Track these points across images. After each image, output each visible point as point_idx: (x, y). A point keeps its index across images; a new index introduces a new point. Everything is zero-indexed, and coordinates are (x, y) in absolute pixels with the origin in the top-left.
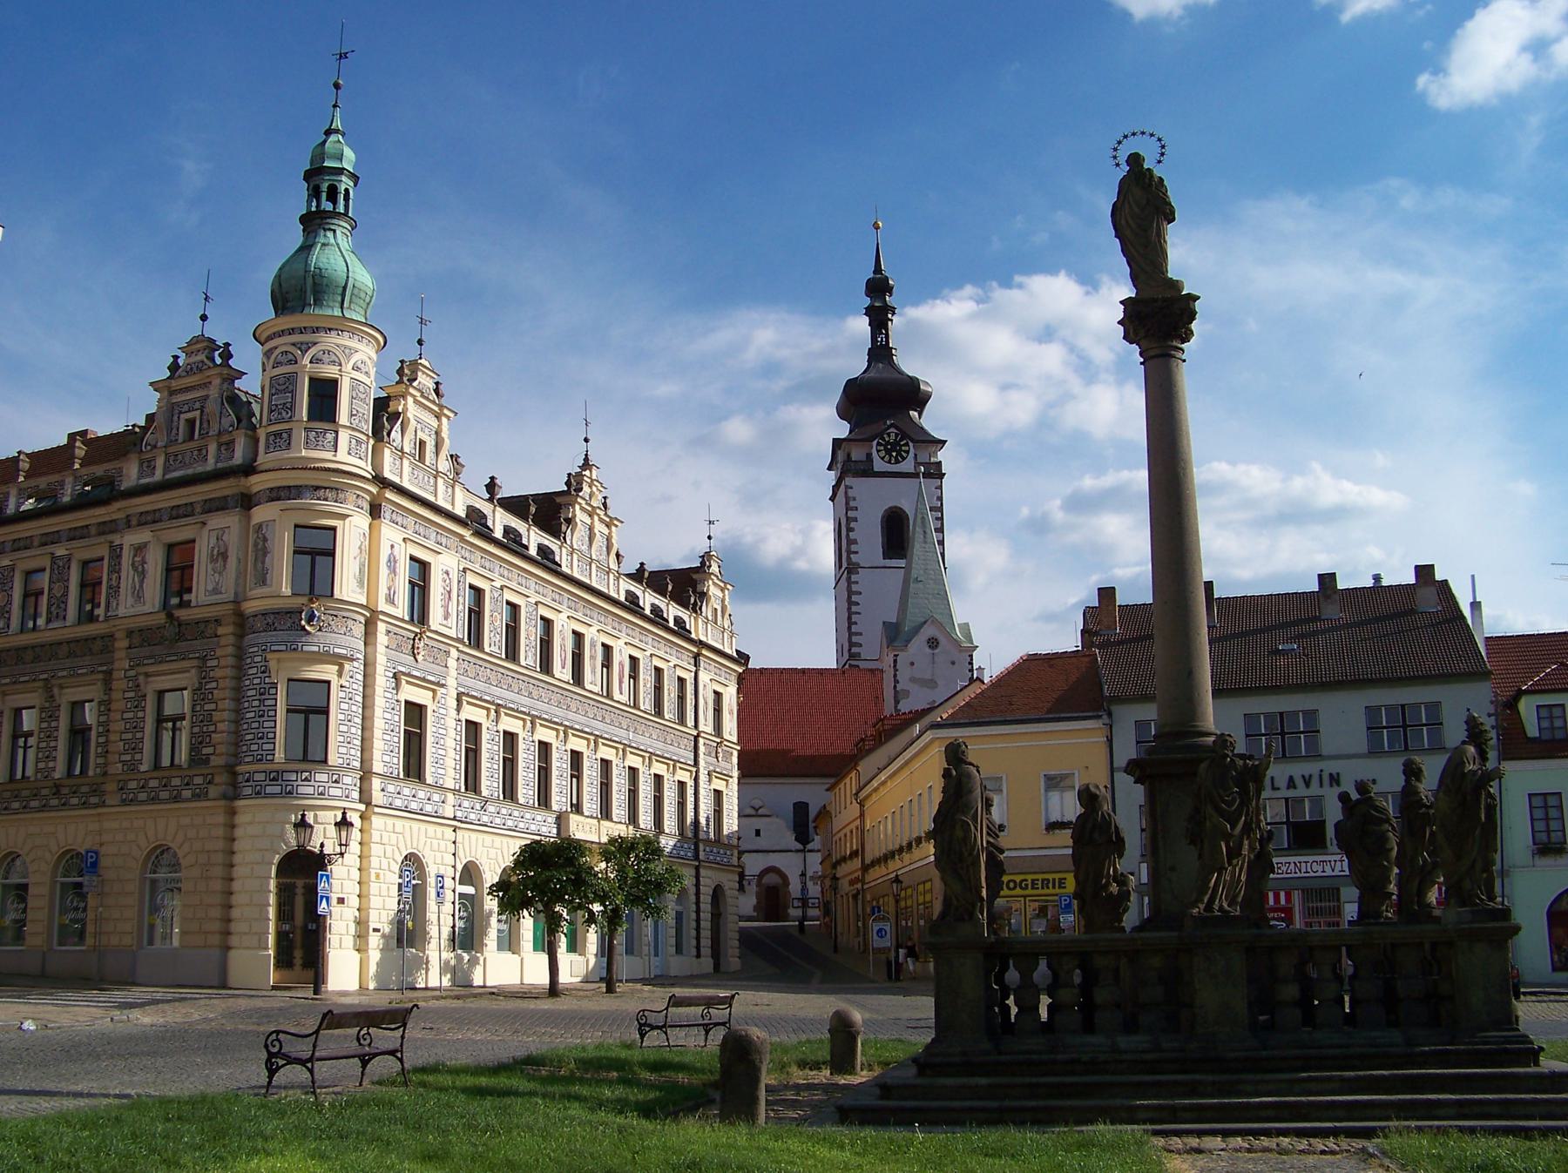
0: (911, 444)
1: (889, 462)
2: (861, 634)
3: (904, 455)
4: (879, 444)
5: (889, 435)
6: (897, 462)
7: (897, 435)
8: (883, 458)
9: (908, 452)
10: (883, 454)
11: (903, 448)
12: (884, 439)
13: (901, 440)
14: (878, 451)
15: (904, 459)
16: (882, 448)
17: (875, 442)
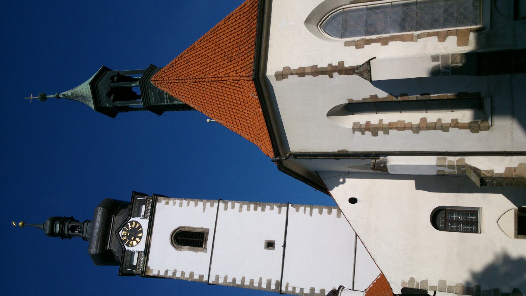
0: (132, 219)
1: (140, 238)
2: (261, 279)
3: (137, 226)
4: (128, 245)
5: (123, 236)
6: (141, 232)
7: (124, 230)
8: (138, 243)
9: (137, 222)
10: (134, 243)
11: (133, 226)
12: (125, 240)
13: (128, 227)
14: (132, 246)
15: (140, 226)
16: (131, 242)
17: (127, 248)
